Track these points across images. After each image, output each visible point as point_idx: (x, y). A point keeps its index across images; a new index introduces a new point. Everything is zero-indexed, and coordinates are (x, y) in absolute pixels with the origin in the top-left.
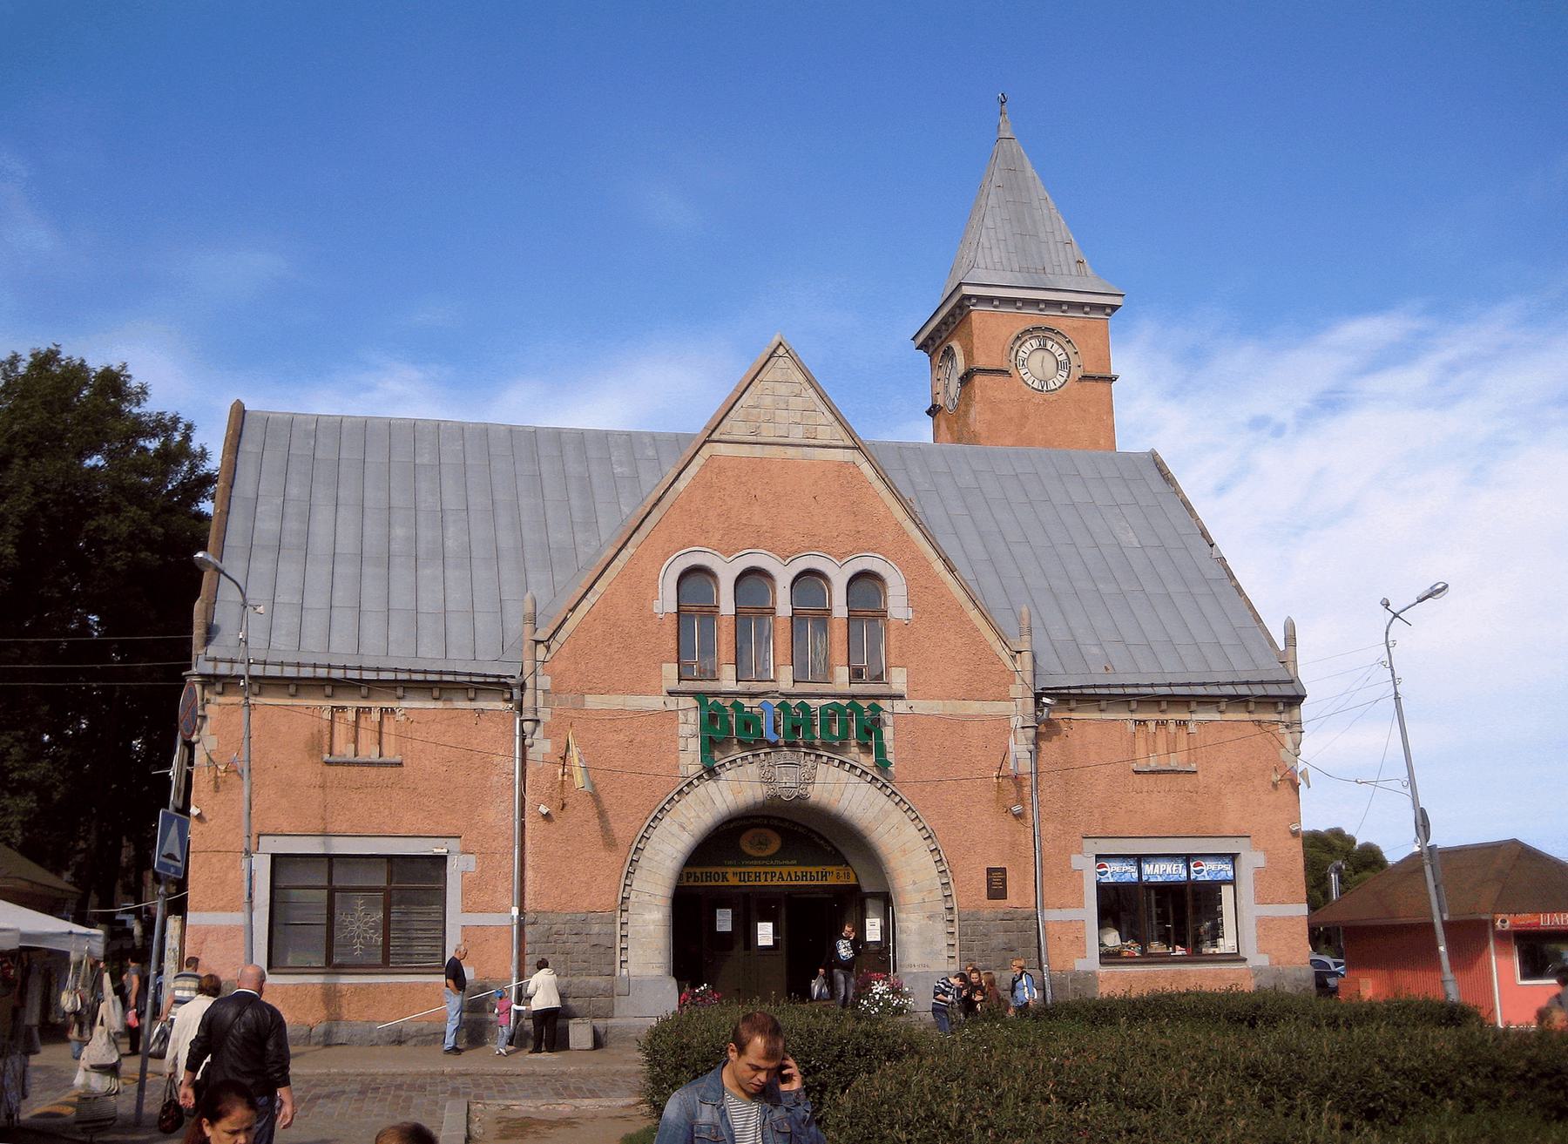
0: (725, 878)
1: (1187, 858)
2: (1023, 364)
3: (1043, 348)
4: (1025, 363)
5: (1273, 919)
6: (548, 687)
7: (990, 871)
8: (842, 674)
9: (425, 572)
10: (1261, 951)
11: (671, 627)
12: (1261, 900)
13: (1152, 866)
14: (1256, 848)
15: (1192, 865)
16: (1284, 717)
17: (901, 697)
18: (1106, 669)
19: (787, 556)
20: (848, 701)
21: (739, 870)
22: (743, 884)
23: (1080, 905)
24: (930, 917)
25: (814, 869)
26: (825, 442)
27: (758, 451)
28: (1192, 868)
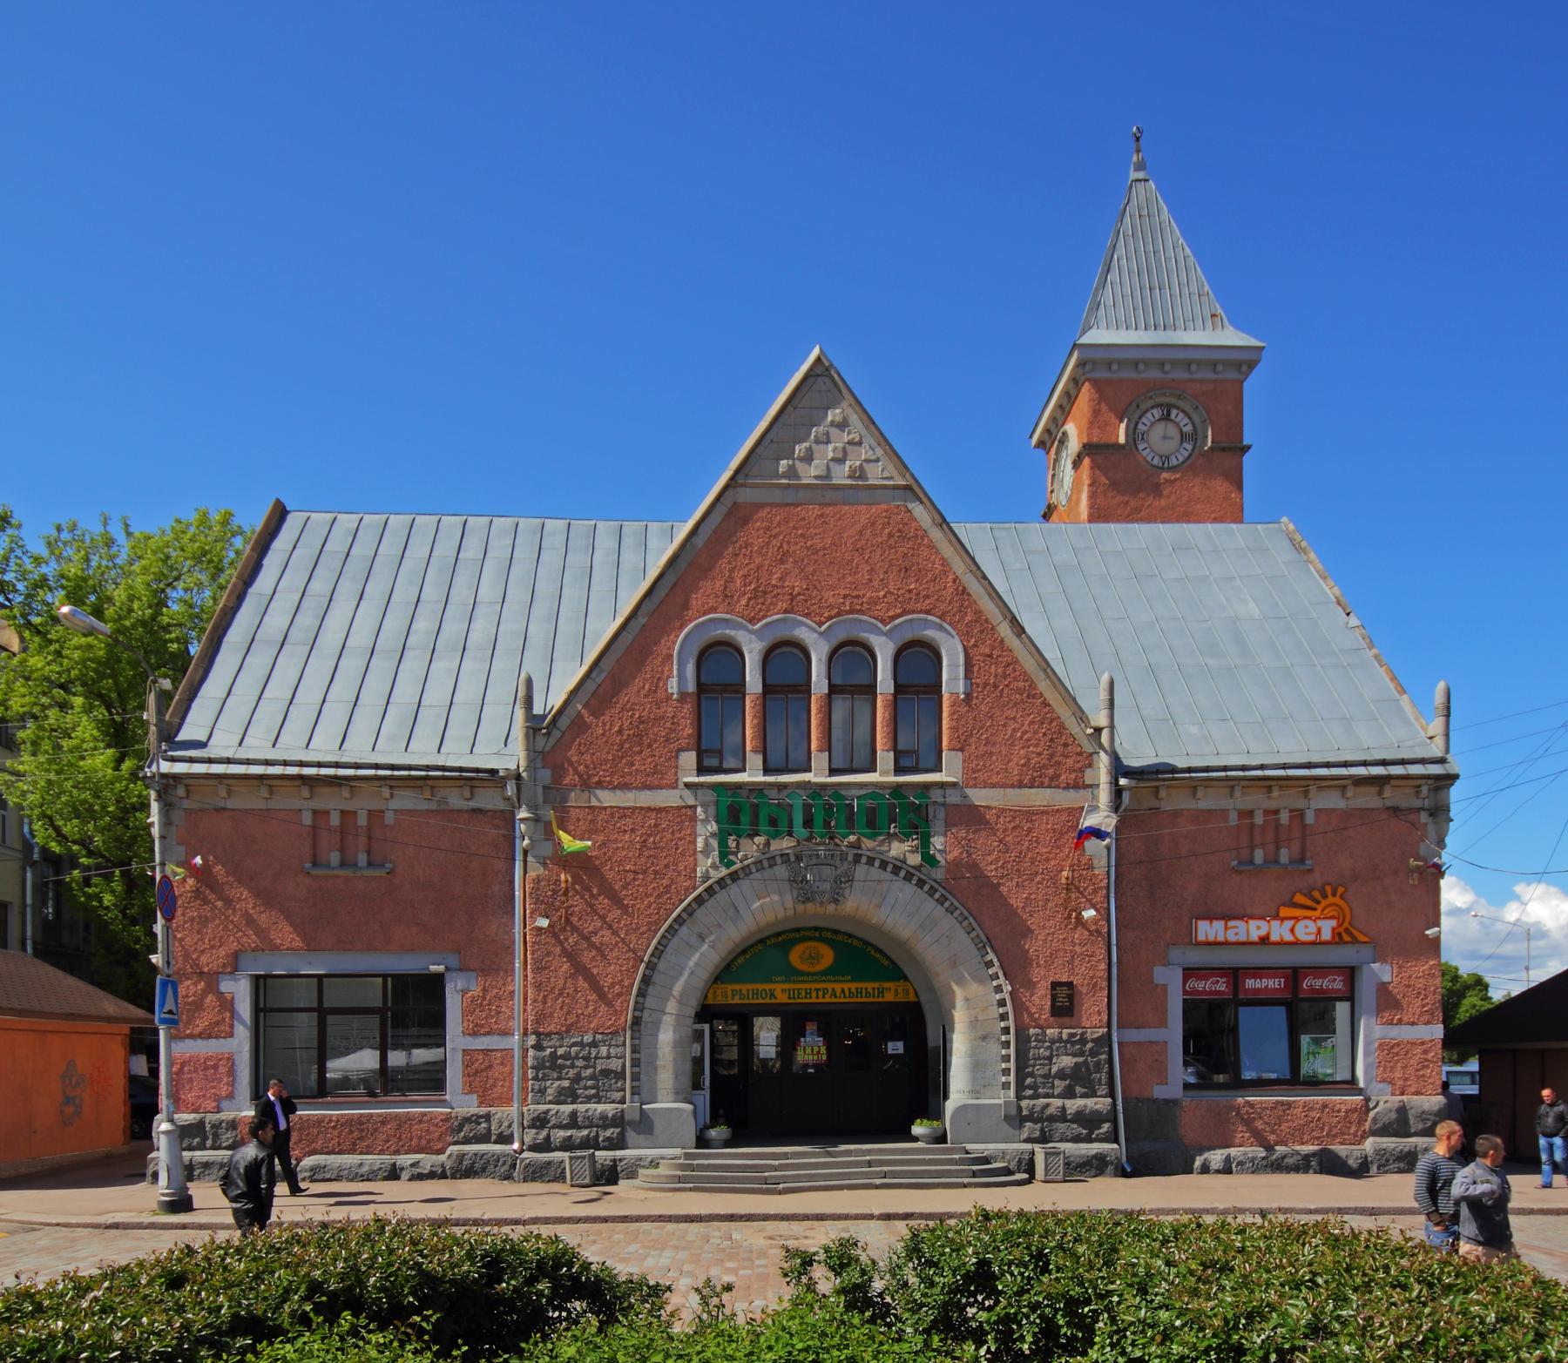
0: (772, 995)
3: (1166, 418)
7: (1055, 985)
21: (786, 986)
24: (984, 1038)
25: (870, 986)
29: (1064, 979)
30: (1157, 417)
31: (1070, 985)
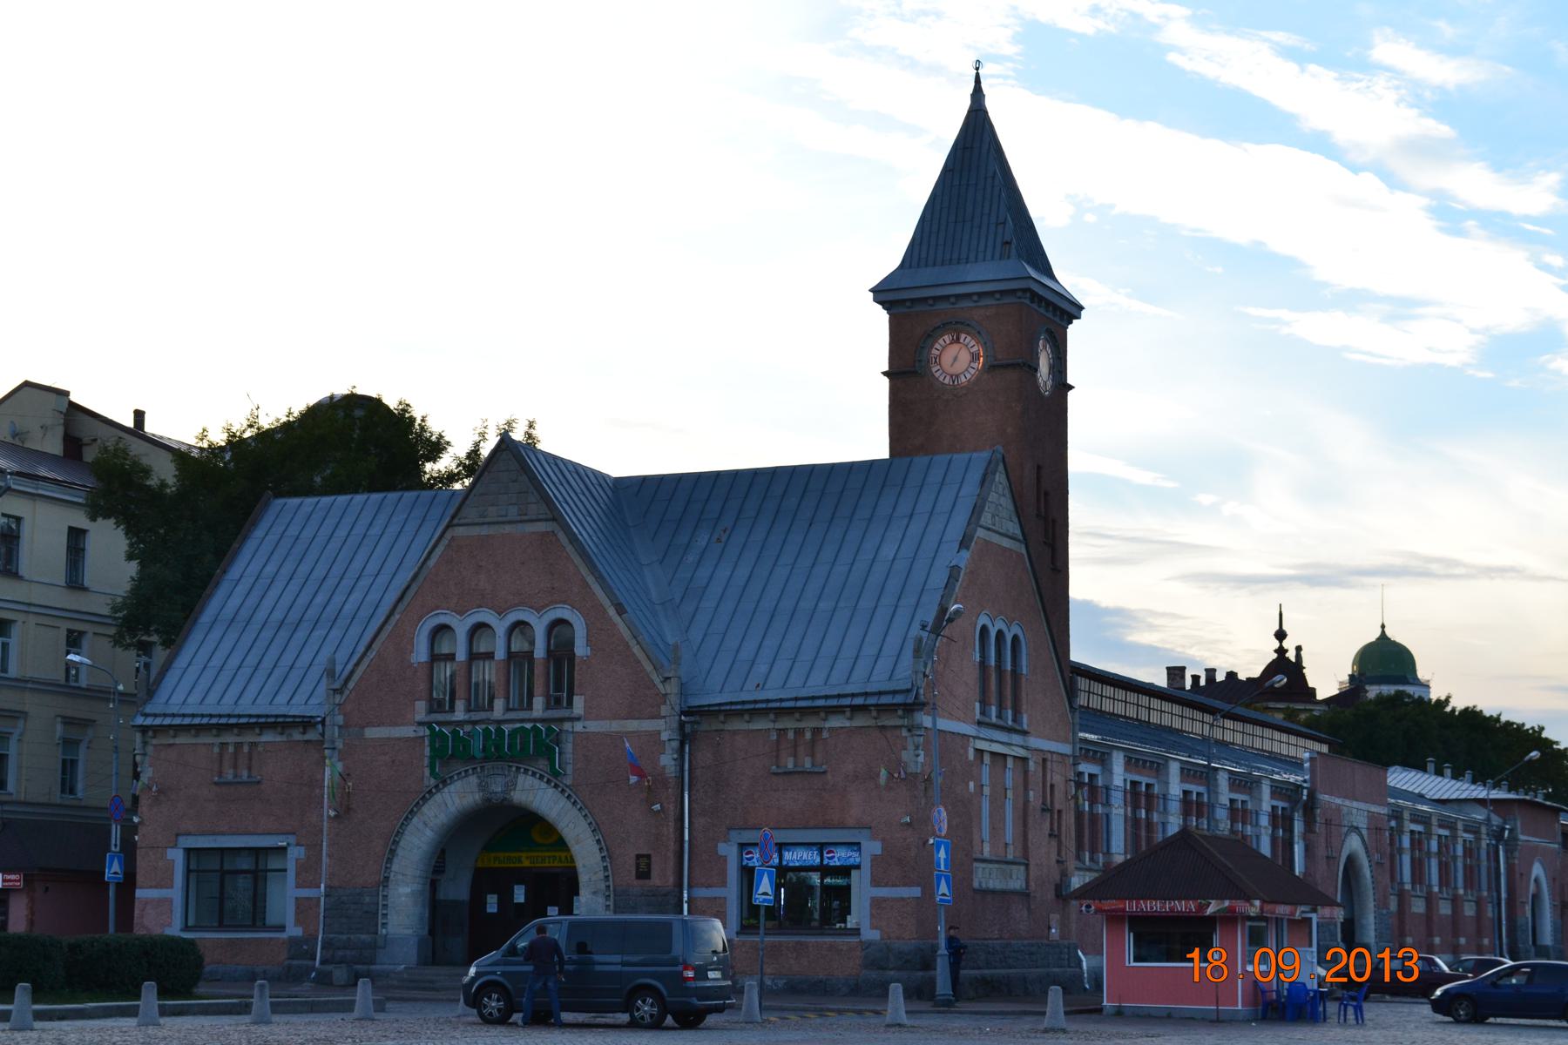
0: (520, 861)
1: (821, 847)
2: (936, 361)
4: (938, 360)
5: (885, 900)
6: (341, 723)
7: (638, 857)
8: (538, 702)
10: (873, 927)
12: (876, 882)
13: (791, 853)
14: (873, 838)
15: (825, 852)
16: (906, 722)
17: (578, 719)
18: (758, 685)
19: (501, 612)
20: (531, 725)
22: (532, 865)
23: (724, 884)
26: (534, 517)
27: (484, 531)
28: (825, 855)
29: (645, 853)
30: (948, 342)
31: (649, 857)
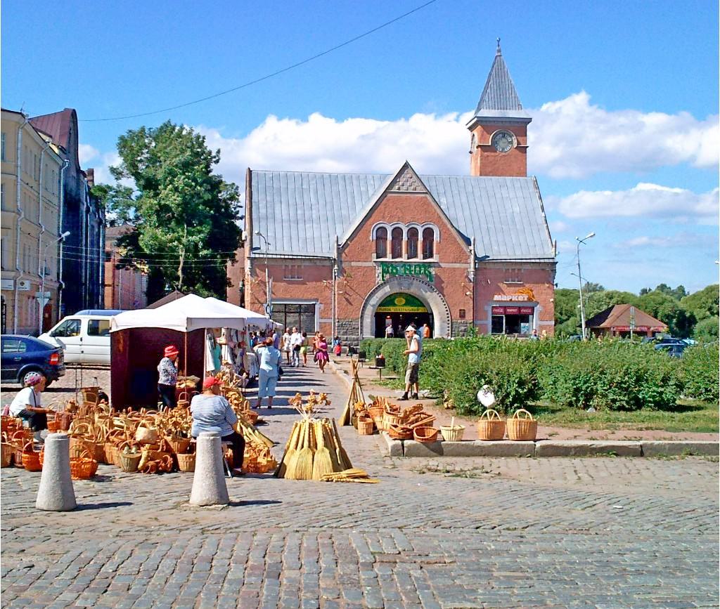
0: (390, 310)
9: (307, 226)
11: (374, 243)
23: (487, 319)
29: (462, 308)
